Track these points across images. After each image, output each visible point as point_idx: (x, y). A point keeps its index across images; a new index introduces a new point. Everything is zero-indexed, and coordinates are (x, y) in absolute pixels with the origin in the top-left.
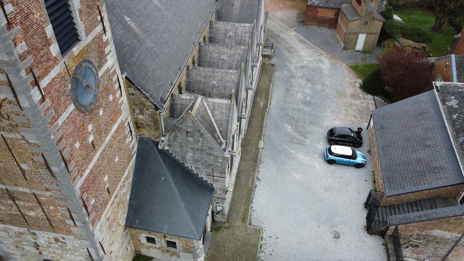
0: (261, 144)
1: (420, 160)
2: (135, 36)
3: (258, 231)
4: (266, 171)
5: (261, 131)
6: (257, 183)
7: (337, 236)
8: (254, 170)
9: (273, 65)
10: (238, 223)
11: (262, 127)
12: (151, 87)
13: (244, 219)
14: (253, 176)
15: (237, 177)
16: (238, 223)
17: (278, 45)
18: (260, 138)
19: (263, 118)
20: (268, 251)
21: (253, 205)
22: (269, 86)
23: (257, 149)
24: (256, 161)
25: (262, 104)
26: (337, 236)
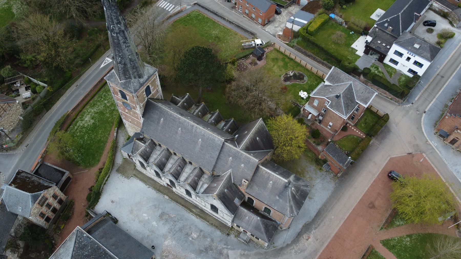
0: (166, 197)
1: (111, 238)
2: (158, 123)
3: (128, 178)
4: (151, 192)
5: (175, 201)
6: (148, 186)
7: (112, 202)
8: (154, 188)
9: (228, 235)
10: (134, 173)
11: (177, 202)
12: (145, 128)
13: (135, 175)
14: (152, 186)
15: (153, 180)
16: (134, 173)
17: (254, 252)
18: (169, 197)
19: (183, 205)
20: (120, 177)
21: (139, 181)
22: (208, 222)
23: (165, 194)
24: (158, 190)
25: (193, 210)
26: (112, 202)
